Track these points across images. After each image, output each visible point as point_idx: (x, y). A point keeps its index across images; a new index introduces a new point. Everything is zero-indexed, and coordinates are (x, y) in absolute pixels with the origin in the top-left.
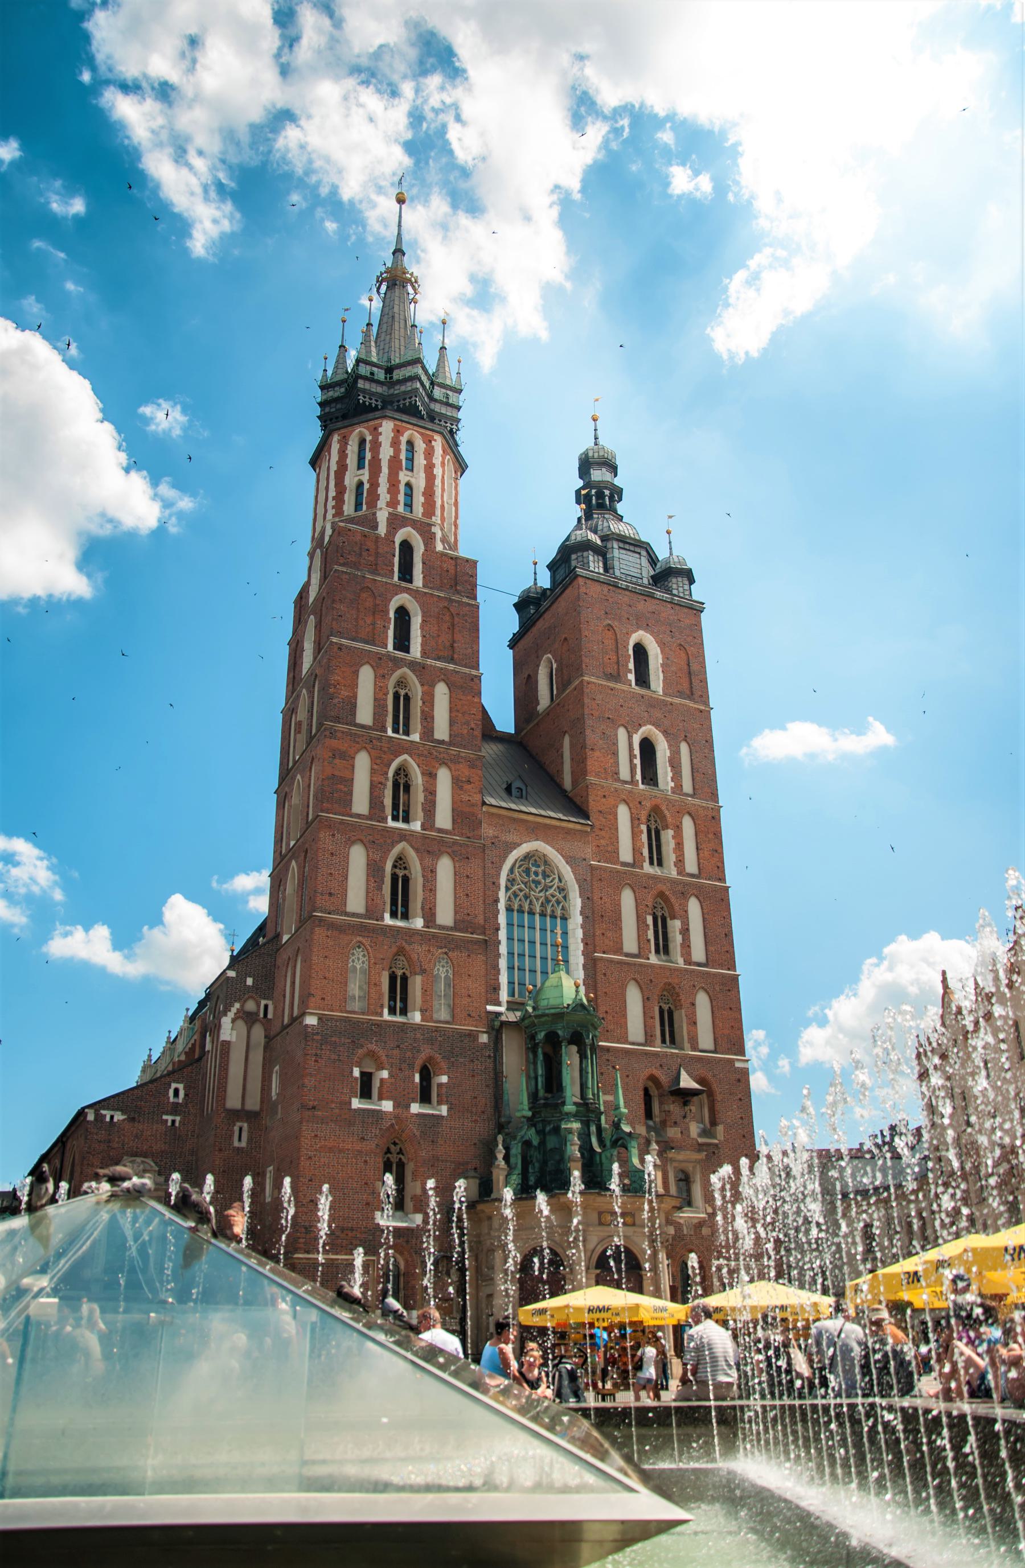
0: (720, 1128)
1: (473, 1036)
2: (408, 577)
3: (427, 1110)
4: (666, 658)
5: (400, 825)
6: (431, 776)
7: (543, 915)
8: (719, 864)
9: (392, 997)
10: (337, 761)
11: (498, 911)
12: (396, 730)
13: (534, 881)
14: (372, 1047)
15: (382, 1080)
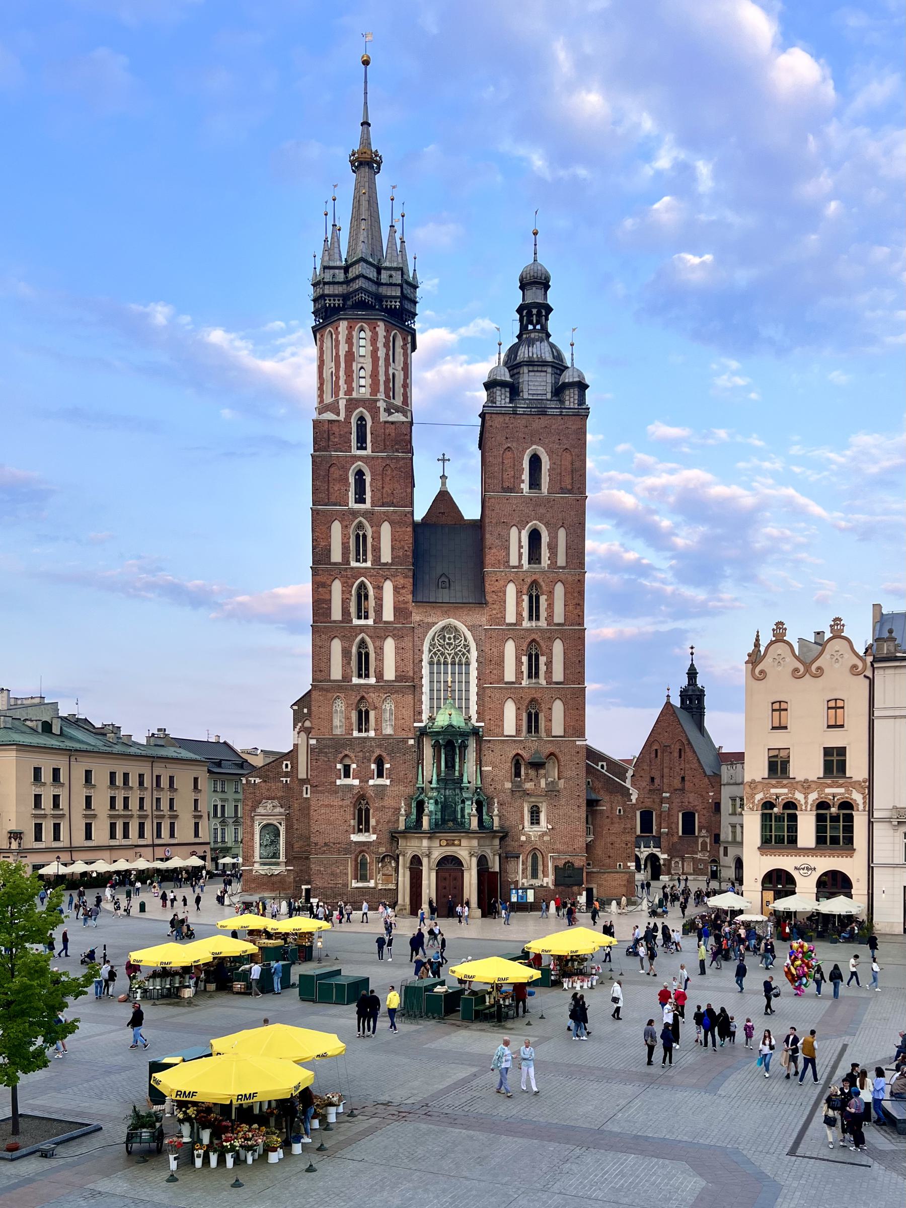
0: (562, 781)
1: (405, 741)
2: (364, 445)
3: (380, 781)
4: (553, 463)
5: (362, 622)
6: (379, 588)
7: (453, 664)
8: (580, 614)
9: (360, 723)
10: (320, 589)
11: (422, 667)
12: (358, 560)
13: (447, 644)
14: (347, 752)
15: (354, 769)
